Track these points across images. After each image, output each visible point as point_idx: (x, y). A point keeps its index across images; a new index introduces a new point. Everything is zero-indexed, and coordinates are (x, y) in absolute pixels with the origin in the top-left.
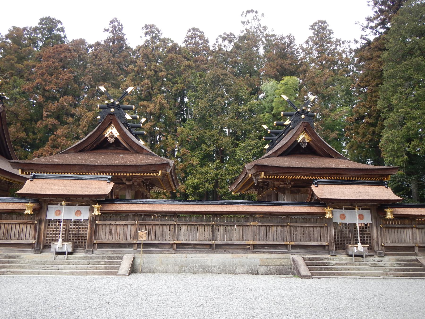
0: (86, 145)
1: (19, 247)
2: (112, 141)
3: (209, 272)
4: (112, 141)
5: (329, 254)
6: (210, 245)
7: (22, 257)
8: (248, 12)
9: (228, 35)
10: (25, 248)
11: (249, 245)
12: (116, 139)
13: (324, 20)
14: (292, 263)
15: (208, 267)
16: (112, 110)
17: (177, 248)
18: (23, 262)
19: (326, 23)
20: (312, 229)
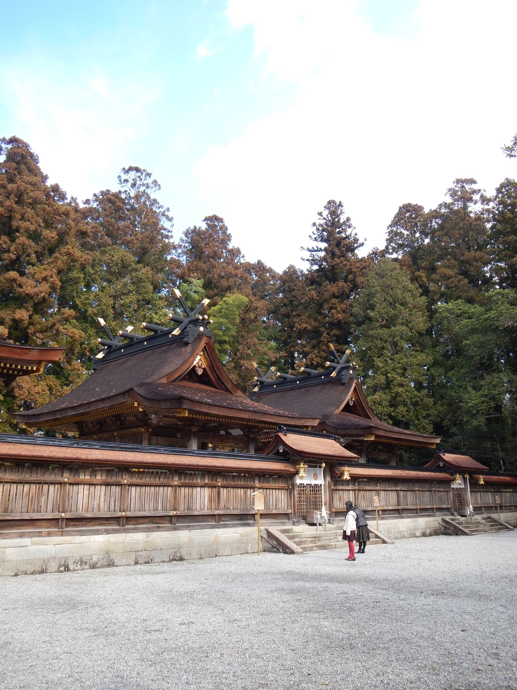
0: (179, 374)
1: (277, 519)
2: (200, 372)
3: (404, 537)
4: (200, 372)
5: (453, 515)
6: (398, 510)
7: (294, 530)
8: (137, 170)
9: (113, 195)
10: (282, 519)
11: (416, 509)
12: (204, 369)
13: (220, 216)
14: (444, 525)
15: (400, 532)
16: (202, 329)
17: (382, 514)
18: (303, 536)
19: (222, 222)
20: (442, 493)
